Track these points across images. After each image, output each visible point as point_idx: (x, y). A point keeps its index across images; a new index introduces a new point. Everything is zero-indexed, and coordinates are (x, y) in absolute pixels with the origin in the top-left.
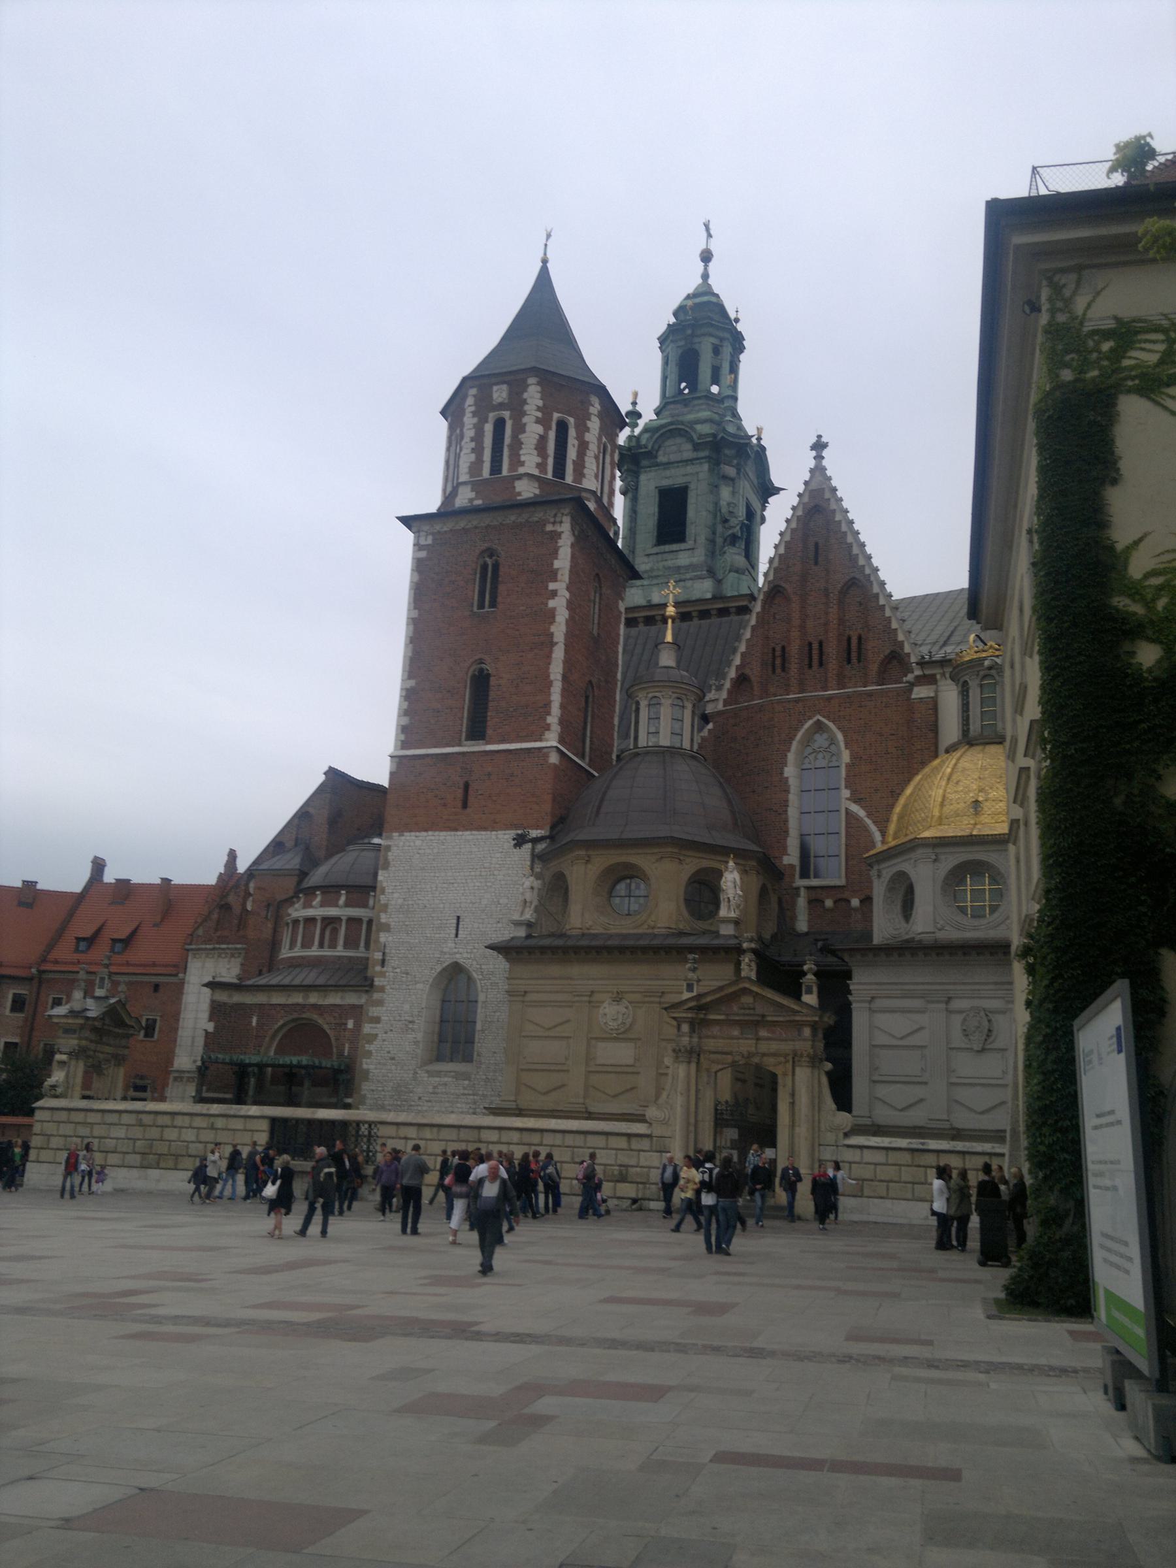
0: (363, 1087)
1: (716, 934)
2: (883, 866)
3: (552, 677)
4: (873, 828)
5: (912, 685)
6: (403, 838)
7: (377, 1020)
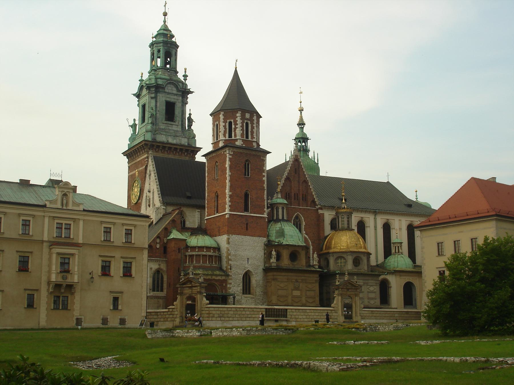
0: (229, 301)
1: (315, 268)
2: (333, 254)
3: (265, 198)
4: (310, 241)
5: (317, 210)
6: (232, 236)
7: (231, 284)
